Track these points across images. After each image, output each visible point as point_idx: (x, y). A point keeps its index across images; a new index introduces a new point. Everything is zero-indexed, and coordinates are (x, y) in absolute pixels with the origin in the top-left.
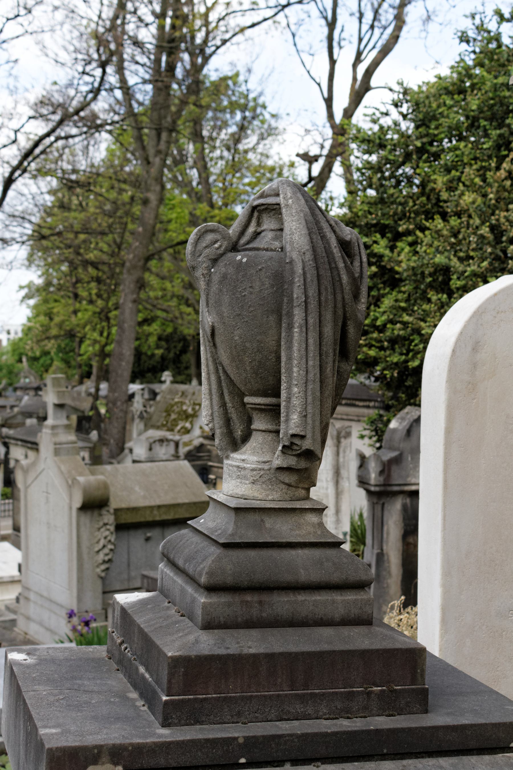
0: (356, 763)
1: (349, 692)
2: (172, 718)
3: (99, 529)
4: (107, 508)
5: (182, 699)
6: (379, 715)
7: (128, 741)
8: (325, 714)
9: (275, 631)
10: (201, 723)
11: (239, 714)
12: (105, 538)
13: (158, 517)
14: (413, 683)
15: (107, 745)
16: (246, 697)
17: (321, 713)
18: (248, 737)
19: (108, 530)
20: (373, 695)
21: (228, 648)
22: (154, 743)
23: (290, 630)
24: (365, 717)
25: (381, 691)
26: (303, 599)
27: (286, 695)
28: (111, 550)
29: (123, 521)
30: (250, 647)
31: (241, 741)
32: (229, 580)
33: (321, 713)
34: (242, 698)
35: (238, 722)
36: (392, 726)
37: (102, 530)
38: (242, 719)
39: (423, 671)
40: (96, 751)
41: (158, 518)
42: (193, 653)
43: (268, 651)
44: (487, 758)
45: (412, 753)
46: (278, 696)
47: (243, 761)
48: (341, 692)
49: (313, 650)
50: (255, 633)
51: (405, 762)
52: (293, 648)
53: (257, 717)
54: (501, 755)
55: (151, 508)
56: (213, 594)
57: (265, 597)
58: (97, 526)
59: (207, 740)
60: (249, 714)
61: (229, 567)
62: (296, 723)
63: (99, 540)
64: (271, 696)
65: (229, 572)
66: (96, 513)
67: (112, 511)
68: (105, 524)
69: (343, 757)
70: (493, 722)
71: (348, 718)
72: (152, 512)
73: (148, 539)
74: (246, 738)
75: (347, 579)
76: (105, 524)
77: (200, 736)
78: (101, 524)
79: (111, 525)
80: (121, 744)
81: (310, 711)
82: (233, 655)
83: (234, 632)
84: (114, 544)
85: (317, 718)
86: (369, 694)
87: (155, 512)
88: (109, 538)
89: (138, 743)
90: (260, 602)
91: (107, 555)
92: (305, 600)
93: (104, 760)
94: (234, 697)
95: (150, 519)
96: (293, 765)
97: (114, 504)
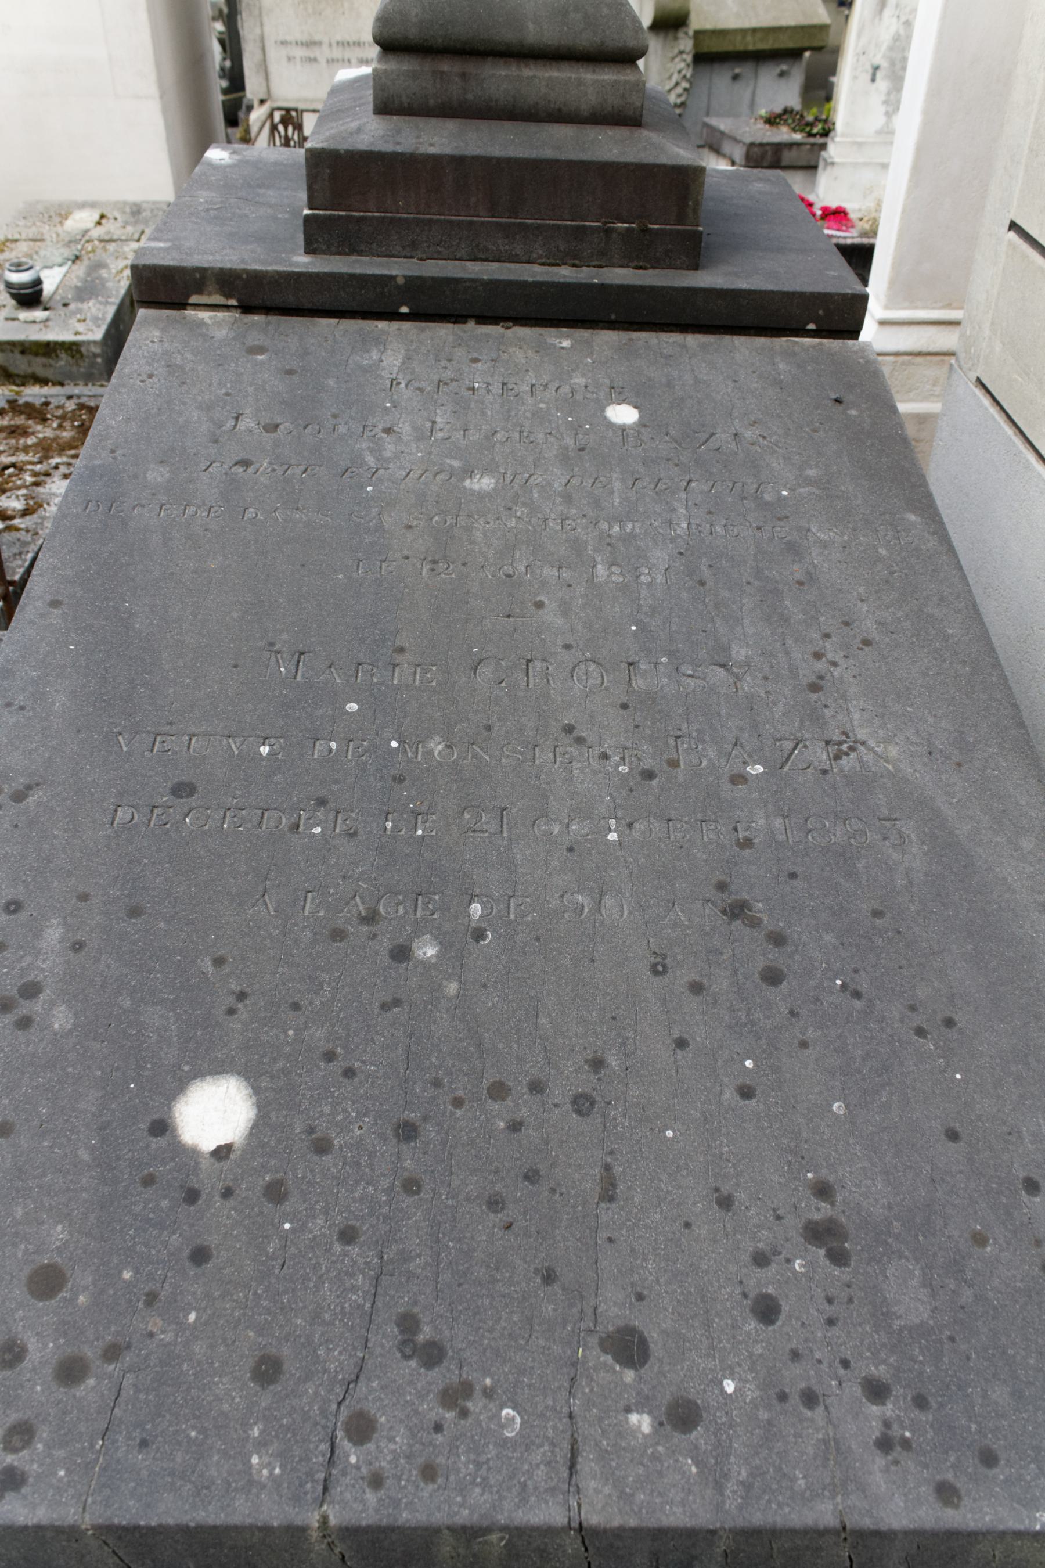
0: (564, 330)
1: (578, 227)
2: (317, 241)
3: (673, 59)
4: (685, 29)
5: (330, 217)
6: (622, 266)
7: (242, 266)
8: (540, 257)
9: (484, 125)
10: (360, 253)
11: (414, 245)
12: (680, 72)
13: (752, 44)
14: (681, 220)
15: (212, 269)
16: (423, 220)
17: (535, 255)
18: (410, 277)
19: (684, 60)
20: (614, 235)
21: (399, 143)
22: (278, 273)
23: (508, 125)
24: (601, 267)
25: (628, 229)
26: (531, 74)
27: (482, 223)
28: (685, 90)
29: (705, 50)
30: (432, 145)
31: (400, 281)
32: (413, 34)
33: (535, 255)
34: (418, 222)
35: (412, 257)
36: (638, 282)
37: (677, 60)
38: (419, 252)
39: (697, 204)
40: (198, 275)
41: (751, 47)
42: (343, 146)
43: (456, 152)
44: (761, 341)
45: (655, 324)
46: (471, 223)
47: (404, 310)
48: (566, 226)
49: (526, 156)
50: (451, 125)
51: (635, 335)
52: (496, 151)
53: (440, 252)
54: (784, 339)
55: (743, 32)
56: (391, 57)
57: (472, 67)
58: (671, 55)
59: (352, 276)
60: (429, 247)
61: (414, 12)
62: (495, 265)
63: (672, 74)
64: (459, 224)
65: (414, 20)
66: (671, 35)
67: (691, 33)
68: (681, 52)
69: (550, 319)
70: (785, 289)
71: (574, 266)
72: (744, 37)
73: (736, 77)
74: (409, 279)
75: (602, 43)
76: (681, 52)
77: (345, 270)
78: (676, 51)
79: (688, 54)
80: (230, 269)
81: (518, 250)
82: (402, 154)
83: (421, 122)
84: (688, 81)
85: (529, 262)
86: (608, 232)
87: (749, 38)
88: (684, 72)
89: (255, 271)
90: (463, 75)
91: (679, 96)
92: (534, 76)
93: (210, 288)
94: (406, 219)
95: (740, 47)
96: (478, 323)
97: (696, 23)
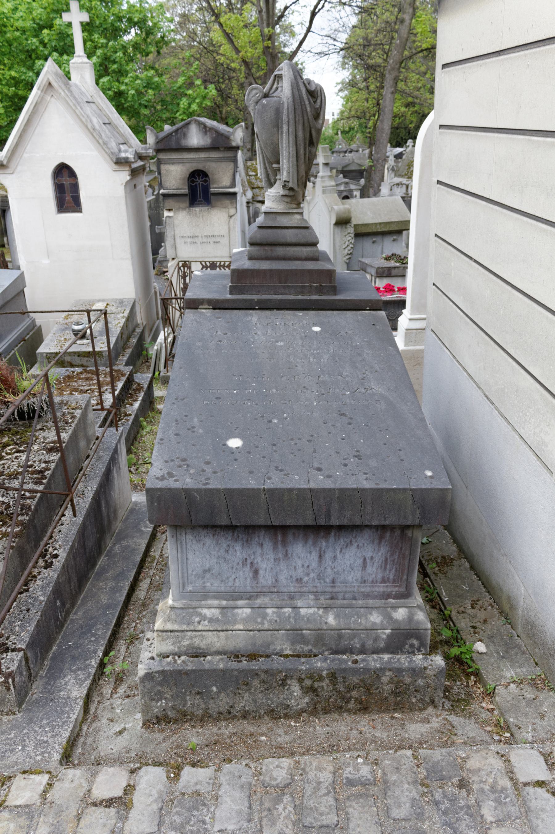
9: (277, 262)
11: (259, 292)
29: (359, 232)
32: (258, 241)
41: (379, 230)
42: (240, 268)
44: (354, 312)
50: (268, 262)
52: (281, 267)
55: (376, 224)
57: (274, 248)
66: (344, 227)
68: (349, 233)
73: (374, 242)
76: (349, 233)
81: (287, 292)
83: (260, 261)
86: (311, 286)
87: (378, 227)
90: (271, 250)
97: (354, 222)
